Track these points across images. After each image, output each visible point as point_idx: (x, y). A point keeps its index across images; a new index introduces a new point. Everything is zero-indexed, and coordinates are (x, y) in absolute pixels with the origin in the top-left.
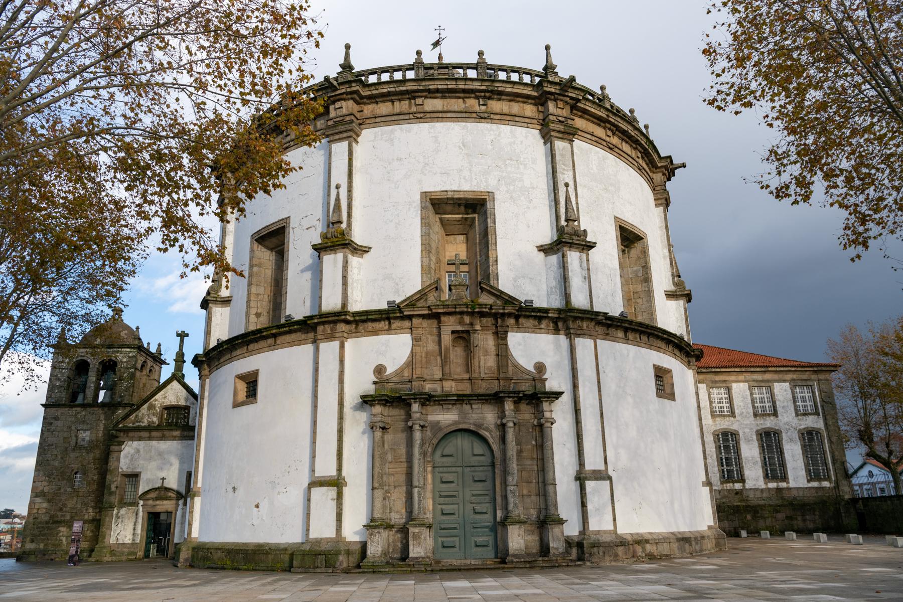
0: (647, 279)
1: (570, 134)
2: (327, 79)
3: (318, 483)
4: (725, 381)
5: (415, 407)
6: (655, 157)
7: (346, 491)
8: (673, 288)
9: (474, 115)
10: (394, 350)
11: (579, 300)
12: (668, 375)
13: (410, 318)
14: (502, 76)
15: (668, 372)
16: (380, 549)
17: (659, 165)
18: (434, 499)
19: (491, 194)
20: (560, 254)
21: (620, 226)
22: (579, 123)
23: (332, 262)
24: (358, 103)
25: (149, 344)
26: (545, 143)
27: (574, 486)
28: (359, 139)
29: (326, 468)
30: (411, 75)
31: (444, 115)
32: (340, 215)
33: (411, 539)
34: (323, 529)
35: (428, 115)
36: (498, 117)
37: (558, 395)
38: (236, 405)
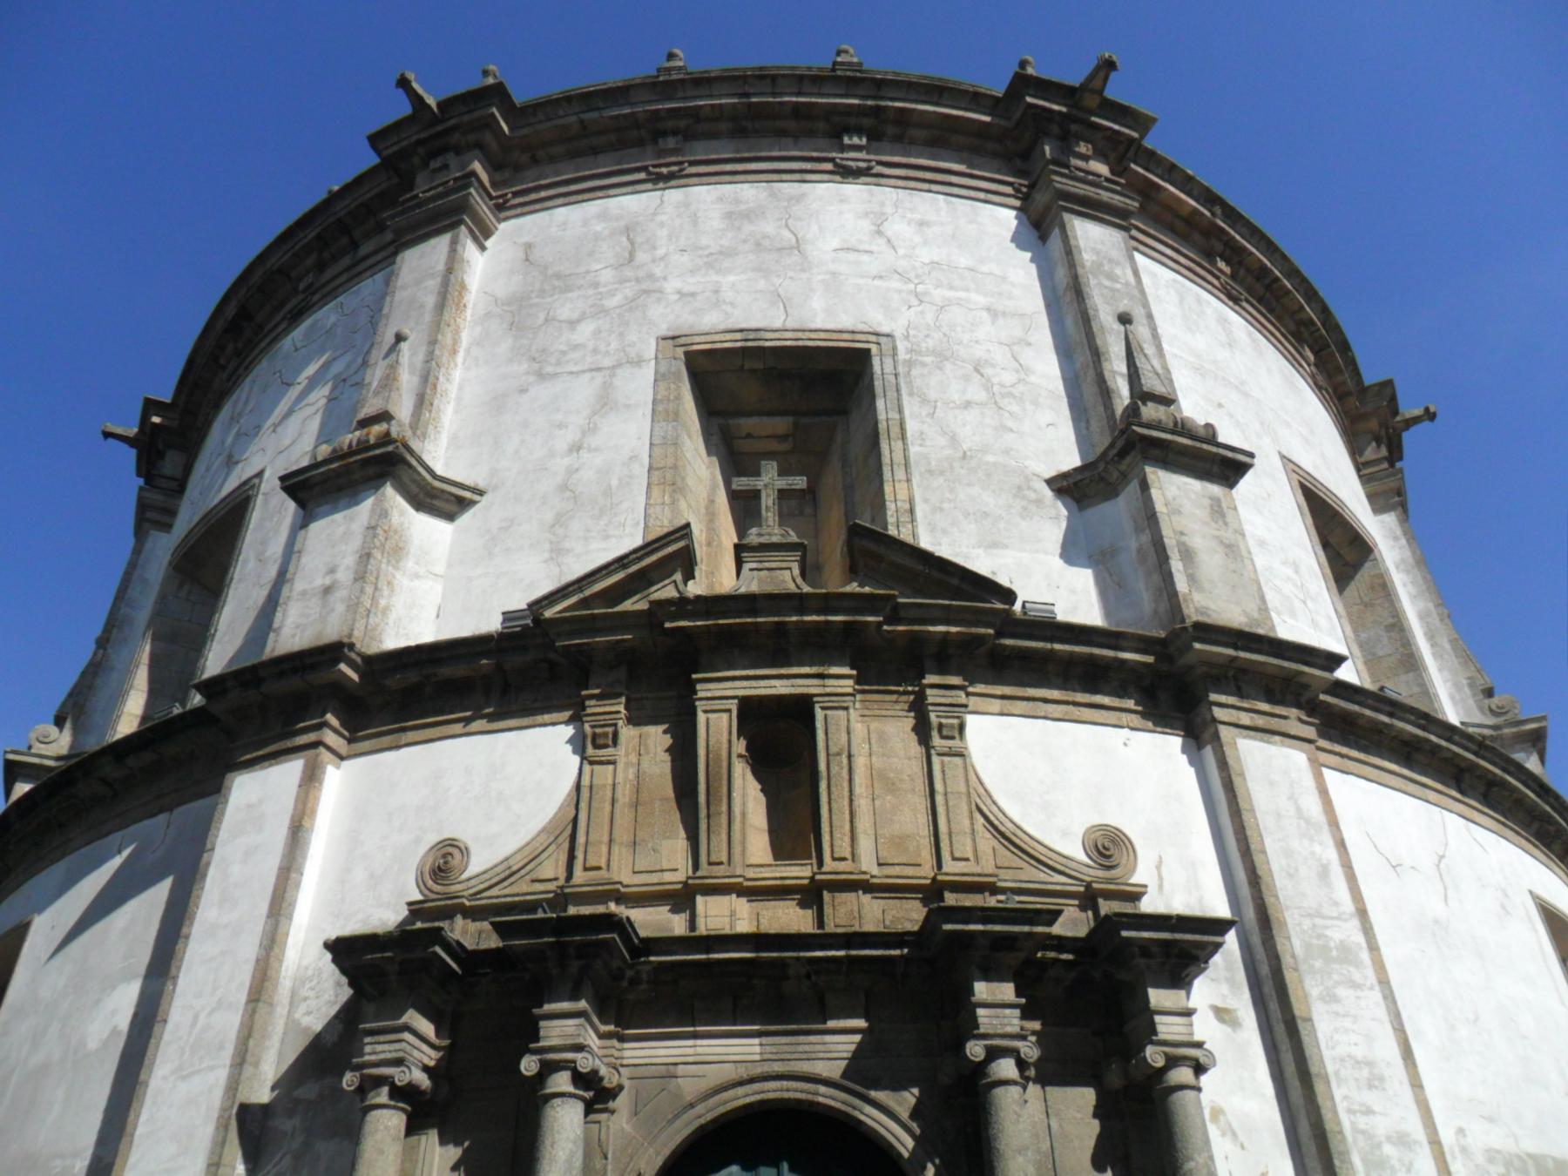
9: (829, 166)
20: (1134, 486)
21: (1302, 486)
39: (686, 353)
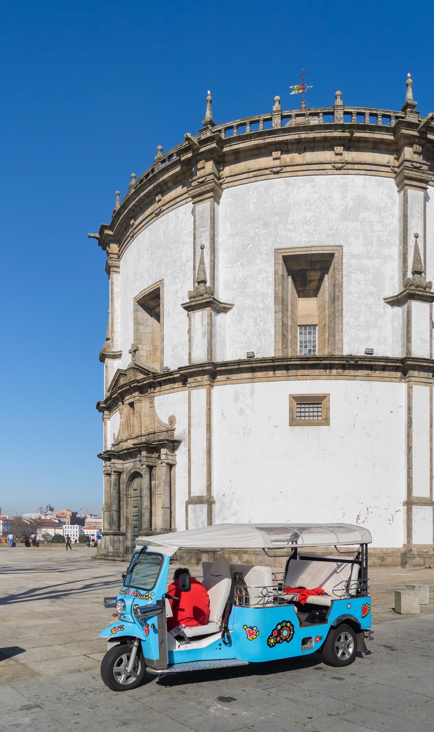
23: (200, 316)
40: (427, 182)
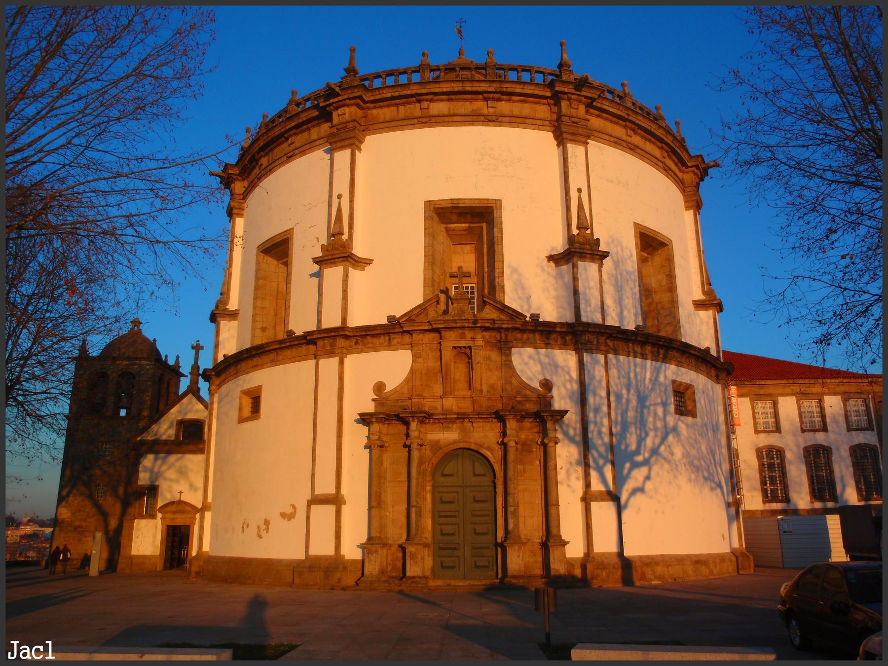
0: (671, 288)
1: (583, 135)
2: (328, 85)
3: (316, 500)
4: (770, 395)
5: (414, 425)
6: (684, 156)
7: (345, 509)
8: (703, 297)
9: (482, 118)
10: (393, 367)
11: (590, 314)
12: (689, 392)
13: (410, 332)
14: (512, 76)
15: (689, 387)
16: (377, 568)
17: (689, 164)
18: (433, 518)
19: (498, 202)
20: (571, 264)
22: (596, 122)
23: (333, 274)
24: (361, 108)
25: (166, 356)
26: (558, 145)
27: (579, 507)
28: (362, 146)
29: (326, 487)
30: (416, 77)
31: (450, 119)
32: (341, 227)
33: (408, 557)
34: (322, 547)
35: (433, 120)
36: (507, 119)
37: (564, 412)
38: (241, 420)
39: (435, 209)
40: (589, 137)
